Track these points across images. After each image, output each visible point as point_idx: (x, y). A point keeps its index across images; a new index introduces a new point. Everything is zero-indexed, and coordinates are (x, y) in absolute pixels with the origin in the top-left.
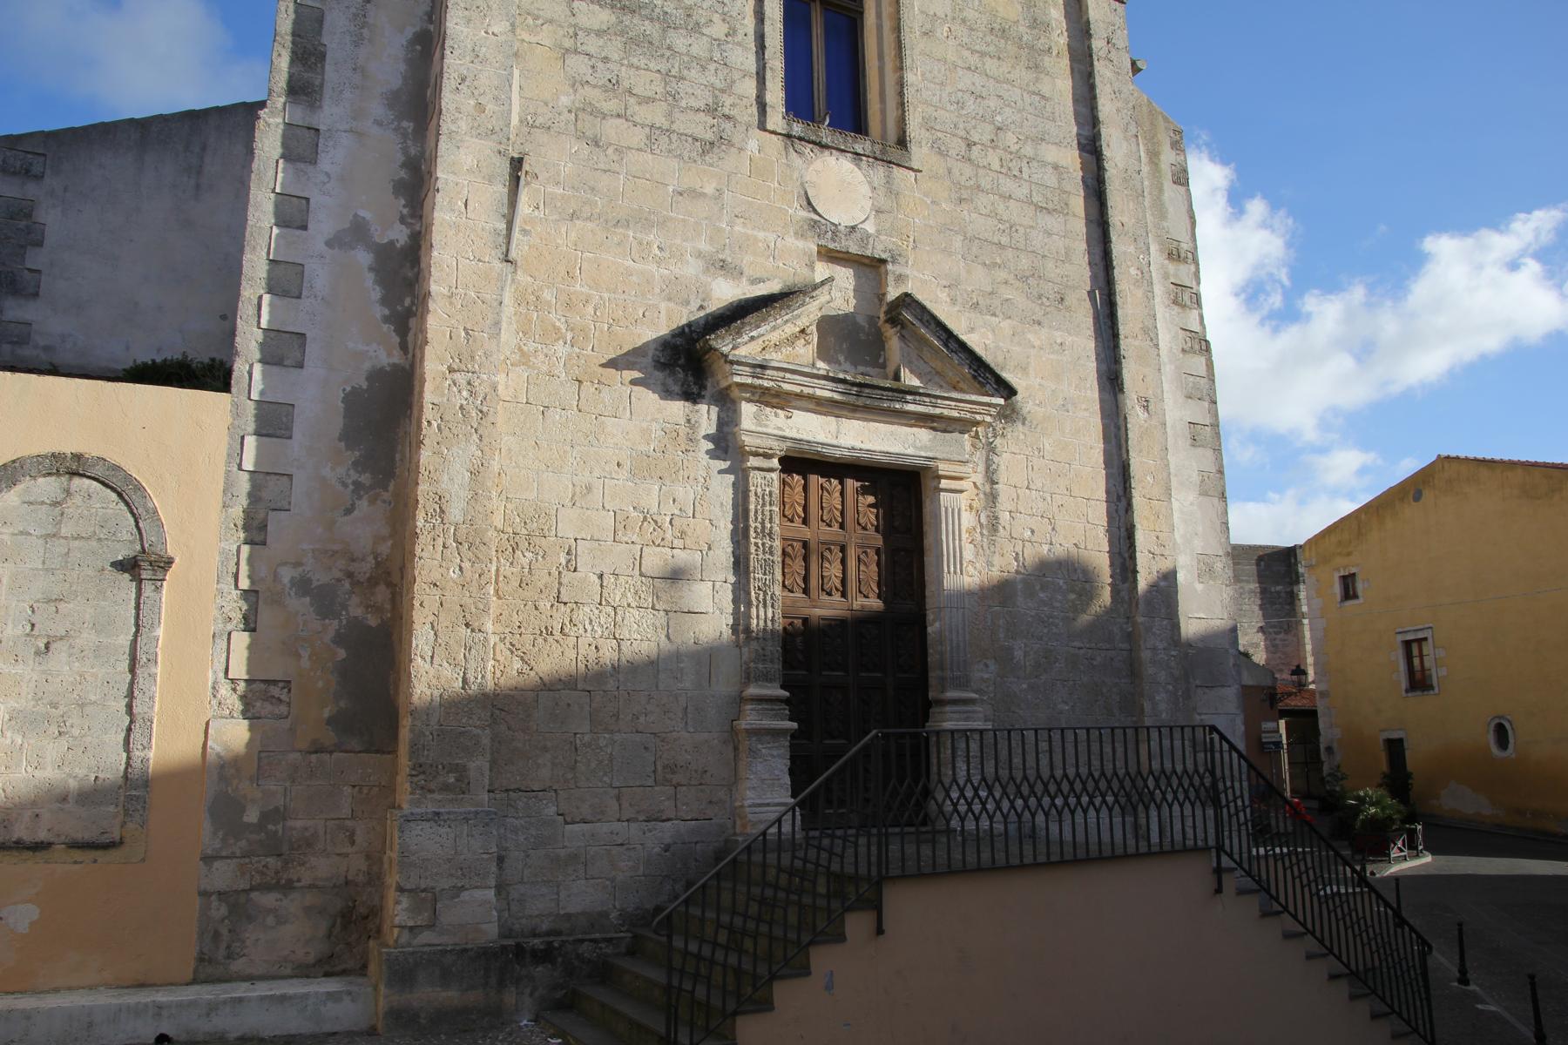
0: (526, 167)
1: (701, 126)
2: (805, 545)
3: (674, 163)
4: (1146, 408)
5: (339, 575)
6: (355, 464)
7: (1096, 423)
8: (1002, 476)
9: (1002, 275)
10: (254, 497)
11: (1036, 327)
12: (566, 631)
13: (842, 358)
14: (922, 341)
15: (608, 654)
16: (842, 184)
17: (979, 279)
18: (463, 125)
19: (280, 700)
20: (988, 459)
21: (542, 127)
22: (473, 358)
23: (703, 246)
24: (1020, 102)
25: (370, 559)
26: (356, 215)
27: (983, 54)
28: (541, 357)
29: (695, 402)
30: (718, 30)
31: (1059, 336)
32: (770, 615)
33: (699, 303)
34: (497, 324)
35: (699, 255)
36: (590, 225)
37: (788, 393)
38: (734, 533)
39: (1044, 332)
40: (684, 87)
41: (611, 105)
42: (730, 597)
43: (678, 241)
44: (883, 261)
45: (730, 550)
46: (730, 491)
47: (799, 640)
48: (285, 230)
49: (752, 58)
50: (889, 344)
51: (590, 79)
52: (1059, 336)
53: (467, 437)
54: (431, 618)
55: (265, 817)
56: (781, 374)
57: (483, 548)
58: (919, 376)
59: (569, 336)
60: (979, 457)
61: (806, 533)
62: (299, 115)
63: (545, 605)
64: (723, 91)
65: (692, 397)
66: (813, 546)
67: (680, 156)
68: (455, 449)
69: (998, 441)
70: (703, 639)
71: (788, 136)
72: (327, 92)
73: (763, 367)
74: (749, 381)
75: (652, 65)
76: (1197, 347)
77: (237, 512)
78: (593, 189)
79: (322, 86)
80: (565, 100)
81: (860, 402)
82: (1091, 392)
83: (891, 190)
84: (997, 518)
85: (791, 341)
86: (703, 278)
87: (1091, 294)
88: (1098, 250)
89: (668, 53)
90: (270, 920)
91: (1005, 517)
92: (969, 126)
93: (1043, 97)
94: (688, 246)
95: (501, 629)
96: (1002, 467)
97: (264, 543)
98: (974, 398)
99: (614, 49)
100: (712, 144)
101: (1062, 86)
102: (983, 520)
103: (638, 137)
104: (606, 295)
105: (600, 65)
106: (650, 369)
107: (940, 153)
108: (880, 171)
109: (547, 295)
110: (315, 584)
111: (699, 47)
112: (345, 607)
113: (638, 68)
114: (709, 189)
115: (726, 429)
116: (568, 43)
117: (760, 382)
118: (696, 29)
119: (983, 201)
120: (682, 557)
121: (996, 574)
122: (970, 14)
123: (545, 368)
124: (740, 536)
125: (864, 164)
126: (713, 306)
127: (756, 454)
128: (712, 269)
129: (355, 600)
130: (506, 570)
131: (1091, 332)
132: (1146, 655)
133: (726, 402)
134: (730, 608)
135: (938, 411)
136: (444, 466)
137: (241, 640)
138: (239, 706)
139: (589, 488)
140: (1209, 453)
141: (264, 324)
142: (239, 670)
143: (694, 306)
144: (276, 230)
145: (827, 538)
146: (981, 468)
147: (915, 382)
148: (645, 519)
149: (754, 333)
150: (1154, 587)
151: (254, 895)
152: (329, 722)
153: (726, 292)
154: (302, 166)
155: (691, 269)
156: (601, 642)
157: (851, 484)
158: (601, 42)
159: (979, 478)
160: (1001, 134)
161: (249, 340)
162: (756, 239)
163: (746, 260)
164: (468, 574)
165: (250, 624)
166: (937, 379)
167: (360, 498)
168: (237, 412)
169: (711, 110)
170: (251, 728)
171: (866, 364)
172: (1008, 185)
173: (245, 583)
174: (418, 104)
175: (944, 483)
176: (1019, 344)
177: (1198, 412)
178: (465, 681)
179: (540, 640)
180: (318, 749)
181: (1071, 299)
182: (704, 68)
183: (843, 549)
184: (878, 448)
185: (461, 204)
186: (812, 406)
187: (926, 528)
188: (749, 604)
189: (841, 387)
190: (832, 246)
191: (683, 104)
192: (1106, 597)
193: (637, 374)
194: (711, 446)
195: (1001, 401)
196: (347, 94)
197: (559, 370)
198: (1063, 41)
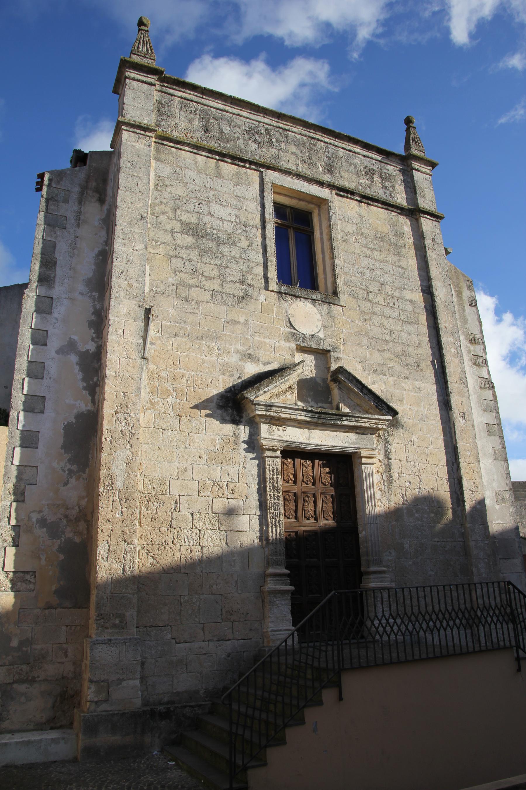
0: (152, 312)
1: (237, 290)
2: (295, 494)
3: (225, 308)
4: (464, 417)
5: (61, 516)
6: (69, 461)
7: (438, 426)
8: (393, 455)
9: (388, 355)
10: (19, 478)
11: (406, 380)
12: (175, 542)
13: (310, 400)
14: (350, 390)
15: (197, 554)
16: (307, 315)
17: (376, 358)
18: (122, 294)
19: (30, 582)
20: (385, 447)
21: (160, 293)
22: (127, 406)
23: (240, 348)
24: (392, 271)
25: (77, 508)
26: (70, 338)
27: (372, 249)
28: (161, 405)
29: (237, 424)
30: (244, 243)
31: (418, 384)
32: (278, 531)
33: (238, 375)
34: (139, 389)
35: (238, 352)
36: (184, 339)
37: (284, 419)
38: (259, 490)
39: (410, 382)
40: (228, 271)
42: (258, 522)
43: (227, 345)
44: (329, 351)
45: (257, 498)
46: (256, 468)
47: (294, 543)
48: (36, 346)
50: (332, 391)
51: (183, 269)
52: (418, 384)
53: (125, 446)
54: (107, 538)
55: (22, 643)
56: (280, 409)
57: (133, 501)
58: (349, 407)
59: (175, 394)
60: (381, 446)
61: (295, 488)
62: (43, 291)
63: (164, 529)
64: (247, 273)
65: (236, 422)
66: (299, 494)
67: (227, 305)
68: (118, 452)
69: (390, 438)
70: (245, 545)
71: (280, 293)
72: (57, 280)
73: (271, 406)
74: (264, 413)
75: (212, 262)
76: (487, 386)
77: (10, 486)
78: (185, 322)
79: (54, 277)
80: (171, 280)
81: (320, 421)
82: (436, 411)
83: (331, 316)
84: (391, 477)
85: (284, 392)
86: (240, 363)
87: (432, 362)
88: (435, 341)
89: (220, 256)
90: (23, 699)
91: (395, 476)
92: (367, 284)
93: (403, 268)
94: (232, 347)
95: (142, 543)
96: (393, 451)
97: (23, 501)
98: (377, 417)
99: (194, 255)
100: (242, 298)
101: (411, 262)
102: (385, 478)
103: (206, 296)
104: (192, 373)
105: (187, 262)
106: (215, 409)
107: (354, 297)
108: (325, 307)
109: (164, 374)
110: (49, 521)
111: (235, 252)
112: (63, 533)
113: (206, 263)
114: (242, 320)
115: (253, 437)
116: (172, 253)
117: (270, 413)
118: (234, 244)
119: (376, 319)
120: (233, 503)
121: (392, 505)
122: (365, 231)
123: (163, 410)
124: (262, 491)
125: (317, 304)
126: (245, 377)
127: (269, 450)
128: (244, 359)
129: (69, 529)
130: (145, 512)
131: (433, 381)
132: (472, 544)
133: (253, 424)
134: (258, 528)
135: (359, 424)
136: (113, 461)
137: (11, 551)
138: (9, 585)
139: (186, 470)
140: (497, 439)
141: (25, 392)
142: (10, 566)
143: (236, 377)
144: (31, 347)
145: (306, 490)
146: (382, 452)
147: (347, 410)
148: (214, 484)
149: (266, 389)
150: (474, 508)
151: (15, 686)
152: (56, 592)
153: (251, 370)
154: (44, 315)
155: (234, 359)
156: (193, 547)
157: (317, 463)
158: (188, 252)
159: (381, 457)
160: (383, 287)
161: (18, 400)
162: (265, 342)
163: (261, 354)
164: (125, 515)
165: (16, 543)
166: (358, 408)
167: (71, 477)
168: (11, 436)
169: (242, 282)
170: (15, 597)
171: (322, 402)
172: (388, 311)
173: (13, 522)
174: (100, 285)
175: (364, 460)
176: (398, 389)
177: (490, 418)
178: (124, 570)
179: (162, 548)
180: (49, 607)
181: (423, 365)
182: (238, 262)
183: (314, 496)
184: (330, 444)
185: (121, 332)
186: (296, 425)
187: (356, 483)
188: (268, 526)
189: (310, 415)
190: (303, 345)
191: (228, 279)
192: (449, 514)
193: (208, 412)
194: (246, 446)
195: (391, 418)
196: (67, 281)
197: (170, 411)
198: (411, 241)
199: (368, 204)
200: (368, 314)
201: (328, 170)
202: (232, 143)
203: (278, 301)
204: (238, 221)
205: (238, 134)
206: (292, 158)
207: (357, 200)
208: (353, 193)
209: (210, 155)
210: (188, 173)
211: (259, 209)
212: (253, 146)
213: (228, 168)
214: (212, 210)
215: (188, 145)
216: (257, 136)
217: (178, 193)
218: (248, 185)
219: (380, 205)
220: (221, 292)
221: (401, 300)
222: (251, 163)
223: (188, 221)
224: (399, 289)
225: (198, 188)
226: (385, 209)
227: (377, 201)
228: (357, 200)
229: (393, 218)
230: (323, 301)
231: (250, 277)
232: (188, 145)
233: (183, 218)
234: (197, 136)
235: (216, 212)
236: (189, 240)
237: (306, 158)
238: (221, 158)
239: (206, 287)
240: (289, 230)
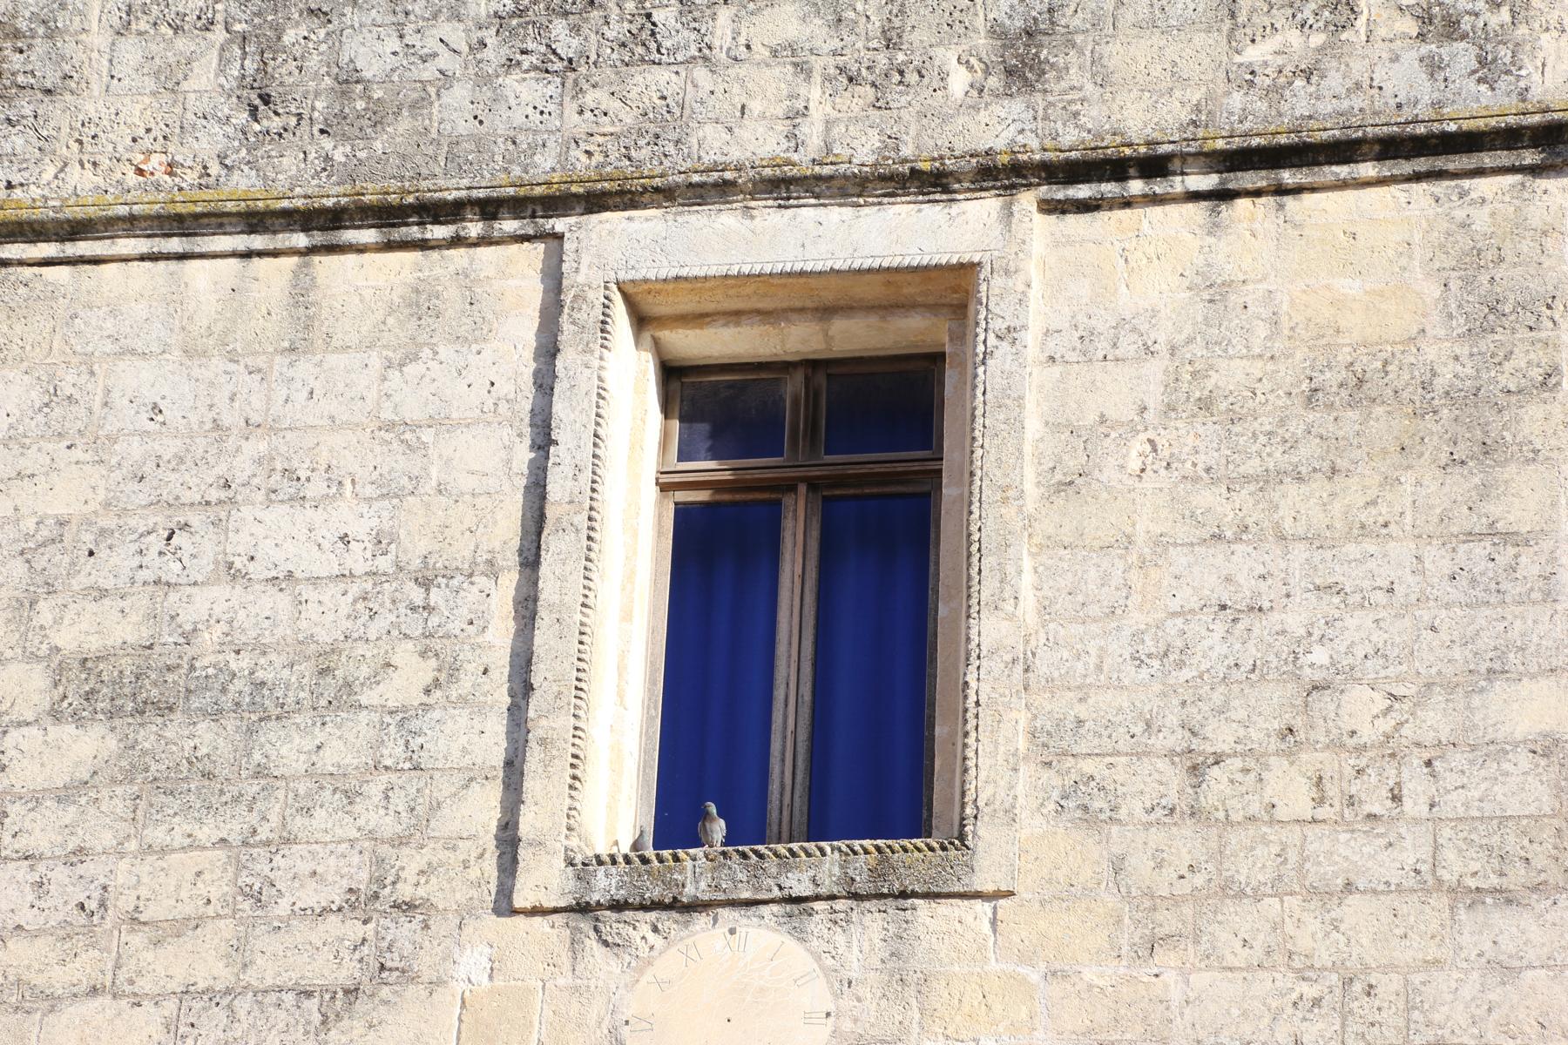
1: (325, 954)
24: (1409, 585)
27: (1267, 481)
30: (410, 676)
40: (296, 860)
41: (86, 966)
49: (497, 727)
64: (400, 841)
71: (582, 908)
89: (253, 788)
93: (1509, 538)
100: (352, 992)
105: (60, 874)
108: (872, 924)
111: (344, 744)
113: (164, 851)
118: (345, 699)
122: (1230, 375)
172: (1341, 852)
182: (351, 796)
191: (283, 908)
199: (1281, 191)
200: (1175, 900)
201: (1009, 72)
202: (405, 124)
203: (565, 959)
204: (384, 564)
205: (445, 61)
206: (769, 87)
207: (1194, 196)
208: (1155, 166)
209: (258, 242)
210: (139, 379)
211: (524, 455)
212: (526, 92)
213: (365, 277)
214: (239, 544)
215: (131, 224)
216: (559, 27)
217: (61, 510)
218: (474, 336)
219: (1368, 170)
220: (228, 991)
221: (1458, 759)
222: (489, 209)
223: (94, 644)
224: (1451, 688)
225: (170, 447)
226: (1417, 177)
227: (1343, 151)
228: (1194, 196)
229: (1481, 220)
230: (855, 896)
231: (411, 862)
232: (131, 224)
233: (68, 639)
234: (210, 151)
235: (266, 550)
236: (88, 745)
237: (860, 48)
238: (319, 238)
239: (145, 985)
240: (788, 500)
